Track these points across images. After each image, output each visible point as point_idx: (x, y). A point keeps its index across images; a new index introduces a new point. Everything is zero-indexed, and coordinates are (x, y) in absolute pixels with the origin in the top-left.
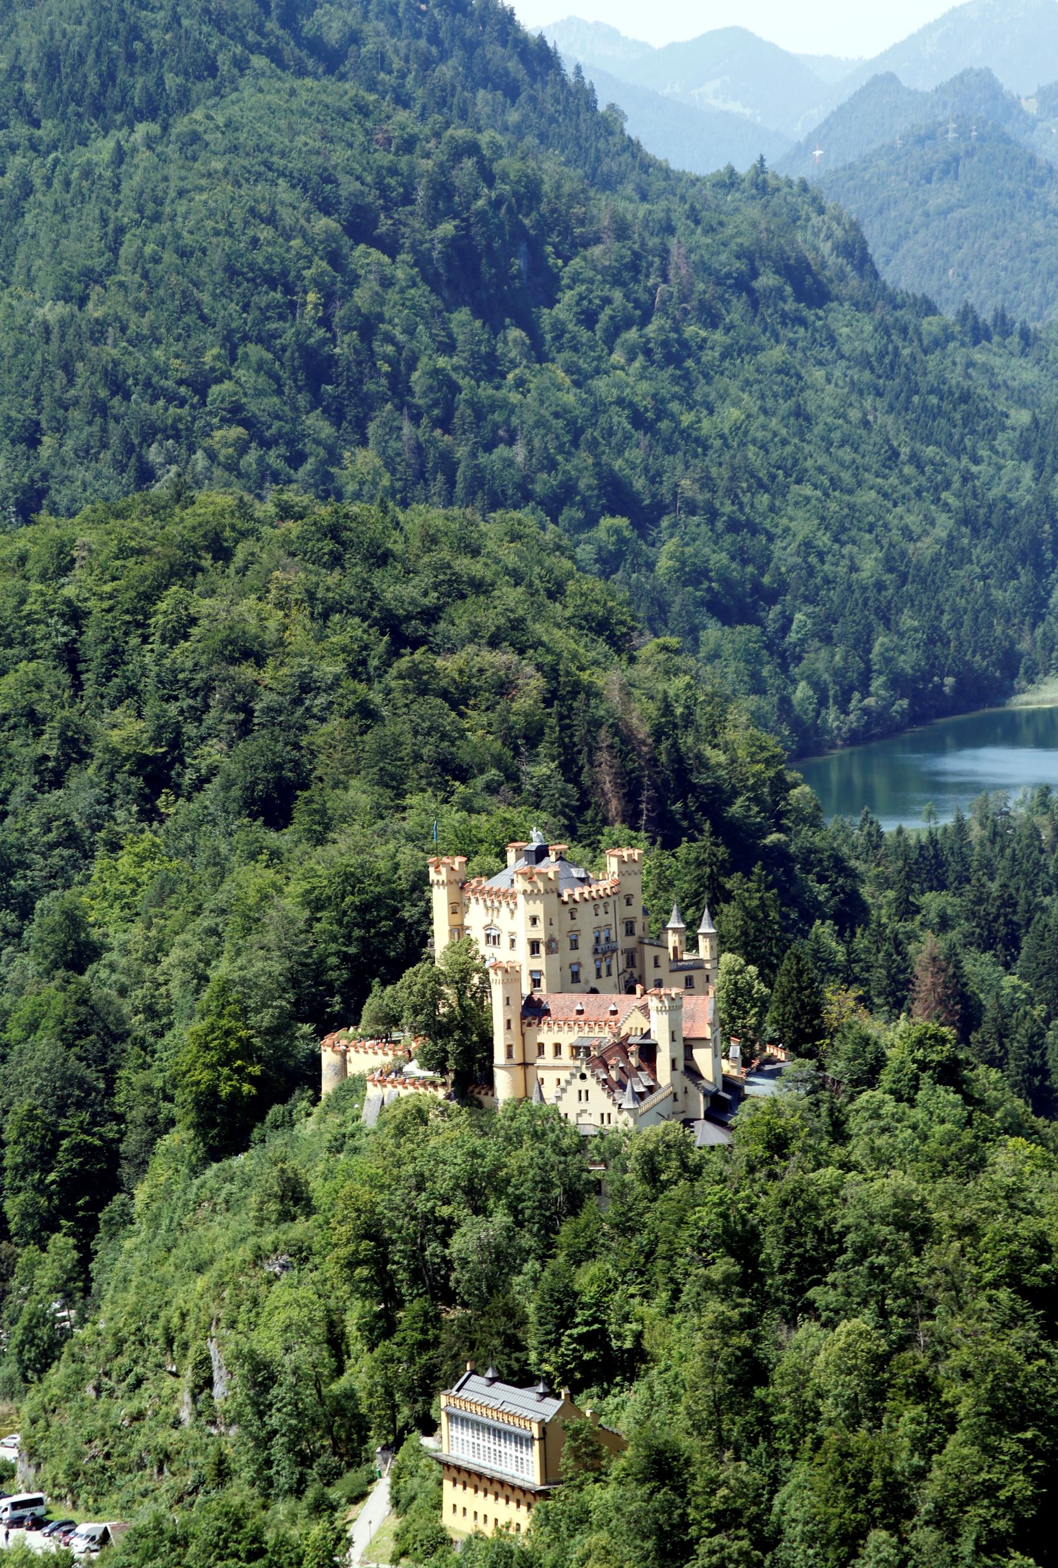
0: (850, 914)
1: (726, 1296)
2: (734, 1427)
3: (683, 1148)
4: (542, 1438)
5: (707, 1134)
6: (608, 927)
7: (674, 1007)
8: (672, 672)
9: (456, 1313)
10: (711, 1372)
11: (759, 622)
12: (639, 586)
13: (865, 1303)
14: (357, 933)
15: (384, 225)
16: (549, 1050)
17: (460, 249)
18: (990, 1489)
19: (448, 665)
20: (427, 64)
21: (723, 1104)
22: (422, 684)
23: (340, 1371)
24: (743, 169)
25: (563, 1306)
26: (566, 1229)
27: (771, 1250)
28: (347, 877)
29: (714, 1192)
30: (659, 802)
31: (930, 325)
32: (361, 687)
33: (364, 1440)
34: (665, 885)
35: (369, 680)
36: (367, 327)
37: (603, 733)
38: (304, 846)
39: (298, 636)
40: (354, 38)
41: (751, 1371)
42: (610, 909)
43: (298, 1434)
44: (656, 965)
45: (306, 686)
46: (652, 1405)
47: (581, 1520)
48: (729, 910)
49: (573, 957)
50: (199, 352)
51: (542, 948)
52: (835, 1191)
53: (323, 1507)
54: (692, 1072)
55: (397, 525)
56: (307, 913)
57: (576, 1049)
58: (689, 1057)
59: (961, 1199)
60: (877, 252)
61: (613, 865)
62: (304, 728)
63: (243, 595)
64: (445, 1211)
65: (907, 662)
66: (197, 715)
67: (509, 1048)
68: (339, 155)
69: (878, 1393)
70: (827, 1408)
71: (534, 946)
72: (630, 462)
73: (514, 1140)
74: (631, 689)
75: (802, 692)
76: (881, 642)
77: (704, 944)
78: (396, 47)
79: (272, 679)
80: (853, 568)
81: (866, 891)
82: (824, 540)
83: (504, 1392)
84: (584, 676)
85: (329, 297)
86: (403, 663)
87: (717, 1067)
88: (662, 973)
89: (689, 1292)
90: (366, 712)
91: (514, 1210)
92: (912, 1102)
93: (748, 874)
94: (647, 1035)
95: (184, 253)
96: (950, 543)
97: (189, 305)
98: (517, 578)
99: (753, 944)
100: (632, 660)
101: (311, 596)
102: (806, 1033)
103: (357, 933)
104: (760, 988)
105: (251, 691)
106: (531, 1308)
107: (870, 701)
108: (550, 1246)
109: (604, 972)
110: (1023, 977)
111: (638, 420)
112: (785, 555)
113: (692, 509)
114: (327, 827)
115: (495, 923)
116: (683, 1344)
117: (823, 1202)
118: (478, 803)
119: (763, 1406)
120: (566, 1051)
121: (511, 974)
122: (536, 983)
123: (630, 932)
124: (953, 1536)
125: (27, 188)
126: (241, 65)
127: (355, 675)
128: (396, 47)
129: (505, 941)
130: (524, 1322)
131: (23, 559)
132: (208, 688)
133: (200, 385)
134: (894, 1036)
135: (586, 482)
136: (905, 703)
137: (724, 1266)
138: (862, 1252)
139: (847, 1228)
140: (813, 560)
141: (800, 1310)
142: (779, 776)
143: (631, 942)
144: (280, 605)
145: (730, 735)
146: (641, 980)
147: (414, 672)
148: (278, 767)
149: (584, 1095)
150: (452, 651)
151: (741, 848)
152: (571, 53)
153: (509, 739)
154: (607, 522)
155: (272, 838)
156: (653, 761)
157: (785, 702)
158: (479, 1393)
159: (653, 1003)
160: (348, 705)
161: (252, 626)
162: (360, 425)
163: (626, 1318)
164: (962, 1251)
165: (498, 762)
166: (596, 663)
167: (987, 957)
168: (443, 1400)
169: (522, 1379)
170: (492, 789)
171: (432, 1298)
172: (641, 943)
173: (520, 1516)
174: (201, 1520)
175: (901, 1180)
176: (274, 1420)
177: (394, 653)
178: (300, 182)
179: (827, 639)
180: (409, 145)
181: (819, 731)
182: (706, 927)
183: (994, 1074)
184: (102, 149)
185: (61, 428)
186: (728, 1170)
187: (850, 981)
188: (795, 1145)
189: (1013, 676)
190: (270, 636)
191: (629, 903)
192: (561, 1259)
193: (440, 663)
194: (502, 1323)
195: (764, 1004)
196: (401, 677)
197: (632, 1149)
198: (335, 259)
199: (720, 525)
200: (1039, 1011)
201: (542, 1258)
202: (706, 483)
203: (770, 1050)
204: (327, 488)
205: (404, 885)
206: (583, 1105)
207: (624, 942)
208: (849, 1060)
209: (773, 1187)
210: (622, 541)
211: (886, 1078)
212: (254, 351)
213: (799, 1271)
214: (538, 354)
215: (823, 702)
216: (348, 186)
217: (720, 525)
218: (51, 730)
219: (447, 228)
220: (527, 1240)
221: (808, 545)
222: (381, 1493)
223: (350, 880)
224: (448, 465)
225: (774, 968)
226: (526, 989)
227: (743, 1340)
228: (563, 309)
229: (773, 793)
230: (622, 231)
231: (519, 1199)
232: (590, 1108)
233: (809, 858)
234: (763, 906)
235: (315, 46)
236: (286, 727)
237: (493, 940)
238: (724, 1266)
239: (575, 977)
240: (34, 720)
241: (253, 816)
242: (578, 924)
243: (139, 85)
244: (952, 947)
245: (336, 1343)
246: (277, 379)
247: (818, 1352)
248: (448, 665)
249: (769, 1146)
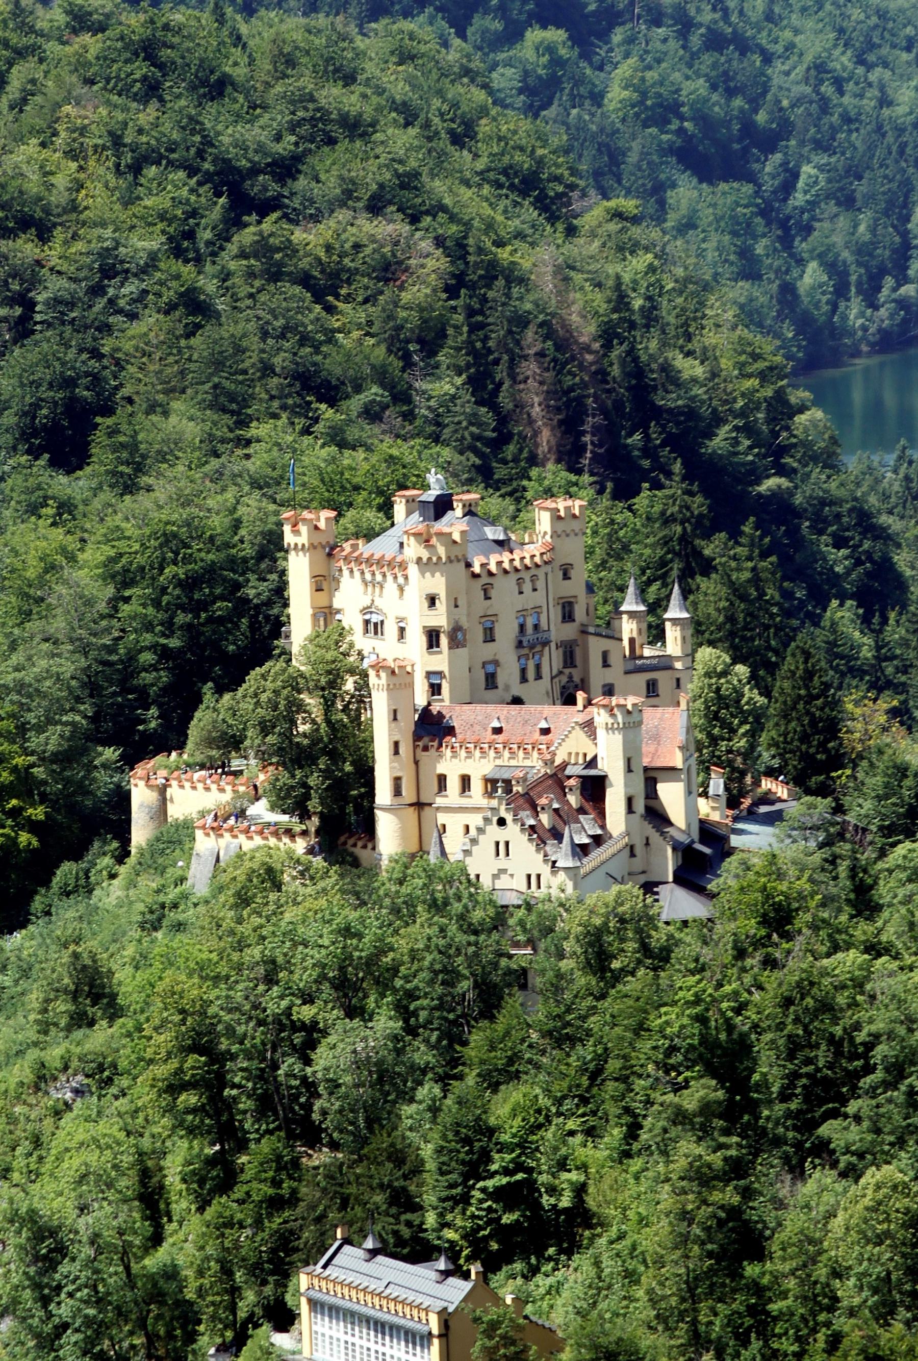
1: (704, 1133)
2: (715, 1319)
3: (642, 923)
4: (444, 1335)
5: (677, 904)
6: (537, 610)
7: (631, 724)
9: (321, 1158)
10: (683, 1241)
11: (751, 178)
12: (581, 127)
13: (901, 1143)
14: (182, 618)
16: (453, 784)
19: (310, 238)
21: (698, 863)
22: (273, 265)
23: (157, 1239)
25: (473, 1147)
26: (477, 1038)
27: (769, 1068)
28: (168, 539)
29: (688, 986)
30: (609, 433)
32: (187, 270)
33: (191, 1337)
34: (618, 550)
35: (198, 260)
38: (107, 495)
39: (98, 198)
41: (739, 1240)
42: (540, 584)
44: (606, 664)
45: (110, 268)
46: (599, 1287)
48: (710, 587)
49: (488, 651)
51: (444, 641)
52: (859, 985)
54: (657, 816)
55: (238, 40)
56: (110, 591)
57: (491, 784)
58: (651, 793)
61: (544, 522)
62: (106, 328)
63: (20, 139)
64: (306, 1013)
67: (397, 781)
70: (848, 1291)
71: (432, 637)
73: (403, 912)
74: (569, 271)
75: (811, 276)
77: (672, 634)
80: (885, 101)
82: (843, 61)
84: (504, 254)
86: (247, 236)
87: (691, 809)
88: (614, 675)
90: (194, 306)
91: (403, 1011)
93: (735, 535)
94: (592, 763)
98: (408, 115)
99: (742, 634)
100: (571, 231)
101: (117, 141)
102: (818, 761)
103: (182, 618)
104: (752, 696)
105: (31, 277)
106: (427, 1151)
108: (455, 1062)
109: (531, 674)
112: (788, 82)
114: (139, 469)
115: (376, 605)
116: (643, 1202)
117: (841, 1000)
118: (353, 433)
119: (757, 1289)
120: (477, 786)
121: (399, 677)
122: (435, 689)
123: (568, 616)
127: (178, 253)
129: (391, 629)
130: (418, 1169)
137: (701, 1091)
138: (897, 1071)
139: (876, 1038)
140: (827, 89)
142: (780, 395)
143: (569, 631)
144: (72, 154)
145: (710, 338)
146: (584, 685)
147: (263, 248)
148: (69, 383)
149: (502, 849)
150: (316, 218)
151: (726, 497)
153: (396, 343)
154: (535, 35)
155: (62, 484)
156: (601, 375)
157: (788, 291)
159: (601, 718)
160: (169, 295)
161: (33, 184)
163: (562, 1165)
165: (381, 376)
166: (519, 235)
168: (304, 1281)
169: (416, 1251)
170: (372, 414)
172: (584, 632)
176: (64, 1310)
177: (233, 222)
179: (848, 202)
182: (675, 611)
186: (707, 954)
187: (880, 686)
188: (802, 919)
191: (566, 576)
192: (471, 1080)
193: (299, 235)
194: (387, 1172)
195: (757, 719)
197: (571, 925)
199: (695, 40)
201: (444, 1080)
203: (767, 784)
205: (248, 551)
206: (502, 863)
207: (560, 632)
208: (879, 798)
210: (557, 62)
213: (807, 1100)
215: (841, 291)
217: (695, 40)
221: (820, 68)
223: (172, 543)
225: (772, 668)
226: (421, 698)
227: (728, 1196)
229: (770, 420)
231: (411, 995)
232: (510, 866)
233: (821, 513)
234: (756, 580)
236: (81, 327)
237: (374, 628)
238: (701, 1091)
239: (491, 681)
241: (34, 453)
242: (495, 605)
245: (151, 1199)
248: (310, 238)
249: (765, 921)
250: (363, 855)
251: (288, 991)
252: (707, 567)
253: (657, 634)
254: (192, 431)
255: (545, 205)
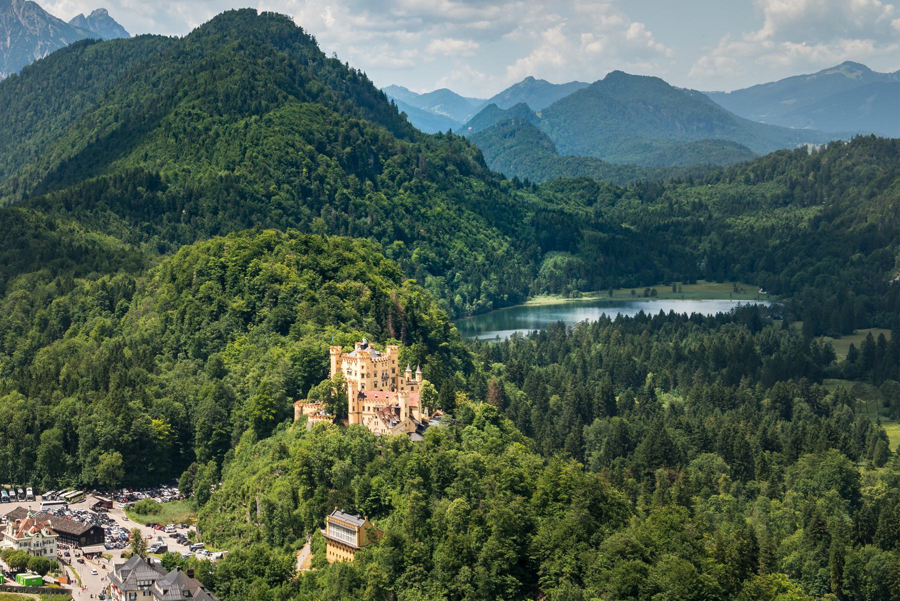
0: (468, 369)
1: (419, 489)
2: (420, 531)
3: (406, 441)
4: (359, 532)
5: (416, 438)
7: (406, 396)
8: (413, 290)
9: (332, 491)
10: (413, 513)
11: (445, 275)
12: (406, 263)
13: (463, 493)
14: (307, 369)
15: (329, 148)
16: (366, 409)
17: (352, 156)
18: (502, 555)
19: (341, 286)
20: (344, 98)
21: (420, 429)
22: (332, 291)
23: (296, 507)
24: (444, 133)
25: (366, 490)
26: (368, 465)
27: (433, 475)
28: (305, 352)
29: (415, 455)
30: (408, 331)
31: (503, 183)
32: (312, 292)
33: (303, 530)
35: (315, 290)
36: (322, 179)
37: (389, 309)
38: (293, 341)
39: (293, 276)
40: (322, 90)
41: (427, 513)
43: (282, 527)
45: (295, 291)
46: (393, 524)
47: (370, 558)
48: (426, 366)
50: (269, 186)
52: (455, 457)
53: (289, 550)
54: (412, 417)
55: (326, 241)
58: (411, 412)
59: (495, 461)
60: (487, 160)
62: (293, 305)
63: (277, 262)
64: (331, 458)
65: (492, 289)
66: (260, 299)
68: (315, 126)
69: (466, 522)
70: (450, 527)
72: (404, 224)
73: (353, 437)
74: (400, 294)
75: (458, 298)
76: (484, 283)
77: (417, 376)
78: (335, 95)
79: (284, 288)
80: (476, 259)
81: (474, 362)
82: (466, 250)
83: (347, 516)
84: (384, 290)
85: (310, 170)
86: (326, 285)
87: (420, 416)
89: (406, 488)
90: (313, 300)
91: (353, 459)
92: (483, 430)
93: (433, 355)
95: (265, 156)
96: (507, 252)
97: (266, 171)
98: (364, 259)
99: (431, 377)
100: (401, 286)
101: (298, 263)
102: (449, 406)
103: (307, 369)
104: (435, 391)
105: (278, 292)
106: (356, 491)
107: (480, 302)
108: (363, 471)
110: (525, 391)
111: (407, 210)
112: (453, 254)
113: (424, 239)
114: (300, 336)
115: (355, 366)
116: (404, 503)
117: (451, 460)
118: (348, 329)
119: (429, 525)
122: (363, 387)
124: (489, 569)
125: (218, 135)
126: (285, 98)
127: (311, 288)
128: (335, 95)
130: (354, 495)
131: (208, 249)
132: (264, 291)
133: (269, 196)
134: (478, 407)
135: (390, 229)
136: (491, 302)
137: (418, 479)
138: (463, 477)
139: (458, 469)
140: (462, 256)
141: (442, 494)
142: (447, 324)
144: (288, 266)
145: (431, 311)
146: (397, 388)
147: (330, 287)
148: (285, 316)
150: (342, 281)
151: (432, 346)
152: (390, 95)
153: (359, 310)
154: (396, 242)
155: (283, 339)
156: (406, 319)
157: (452, 301)
158: (338, 516)
159: (400, 395)
160: (308, 297)
161: (279, 272)
162: (319, 210)
163: (386, 495)
164: (495, 478)
165: (355, 317)
166: (388, 286)
167: (513, 384)
168: (327, 518)
169: (353, 512)
170: (353, 325)
171: (326, 485)
173: (351, 557)
174: (249, 552)
175: (476, 454)
176: (274, 522)
177: (323, 282)
178: (302, 134)
179: (467, 282)
180: (337, 123)
181: (463, 310)
182: (418, 371)
183: (510, 422)
184: (242, 123)
185: (225, 209)
186: (421, 449)
187: (467, 390)
188: (442, 442)
189: (527, 295)
190: (284, 275)
192: (367, 475)
193: (338, 285)
194: (347, 495)
195: (436, 397)
196: (325, 289)
197: (390, 441)
198: (312, 158)
199: (433, 244)
200: (529, 402)
201: (361, 475)
202: (429, 231)
203: (438, 411)
204: (307, 229)
205: (323, 355)
209: (435, 455)
210: (401, 248)
211: (475, 421)
212: (286, 186)
213: (443, 482)
214: (376, 188)
215: (465, 301)
216: (318, 136)
217: (433, 244)
218: (215, 302)
219: (348, 149)
220: (356, 469)
221: (461, 251)
222: (307, 547)
223: (305, 352)
224: (346, 223)
225: (440, 385)
226: (359, 389)
227: (423, 504)
228: (384, 176)
229: (445, 330)
230: (404, 151)
231: (354, 455)
232: (377, 427)
233: (456, 351)
234: (438, 365)
235: (309, 93)
236: (288, 304)
238: (418, 479)
239: (376, 386)
240: (210, 299)
241: (277, 332)
242: (377, 369)
243: (254, 104)
244: (501, 381)
245: (295, 499)
246: (293, 195)
247: (449, 508)
248: (341, 286)
249: (434, 442)
250: (346, 424)
251: (328, 453)
252: (426, 362)
253: (414, 377)
254: (313, 328)
255: (394, 280)
